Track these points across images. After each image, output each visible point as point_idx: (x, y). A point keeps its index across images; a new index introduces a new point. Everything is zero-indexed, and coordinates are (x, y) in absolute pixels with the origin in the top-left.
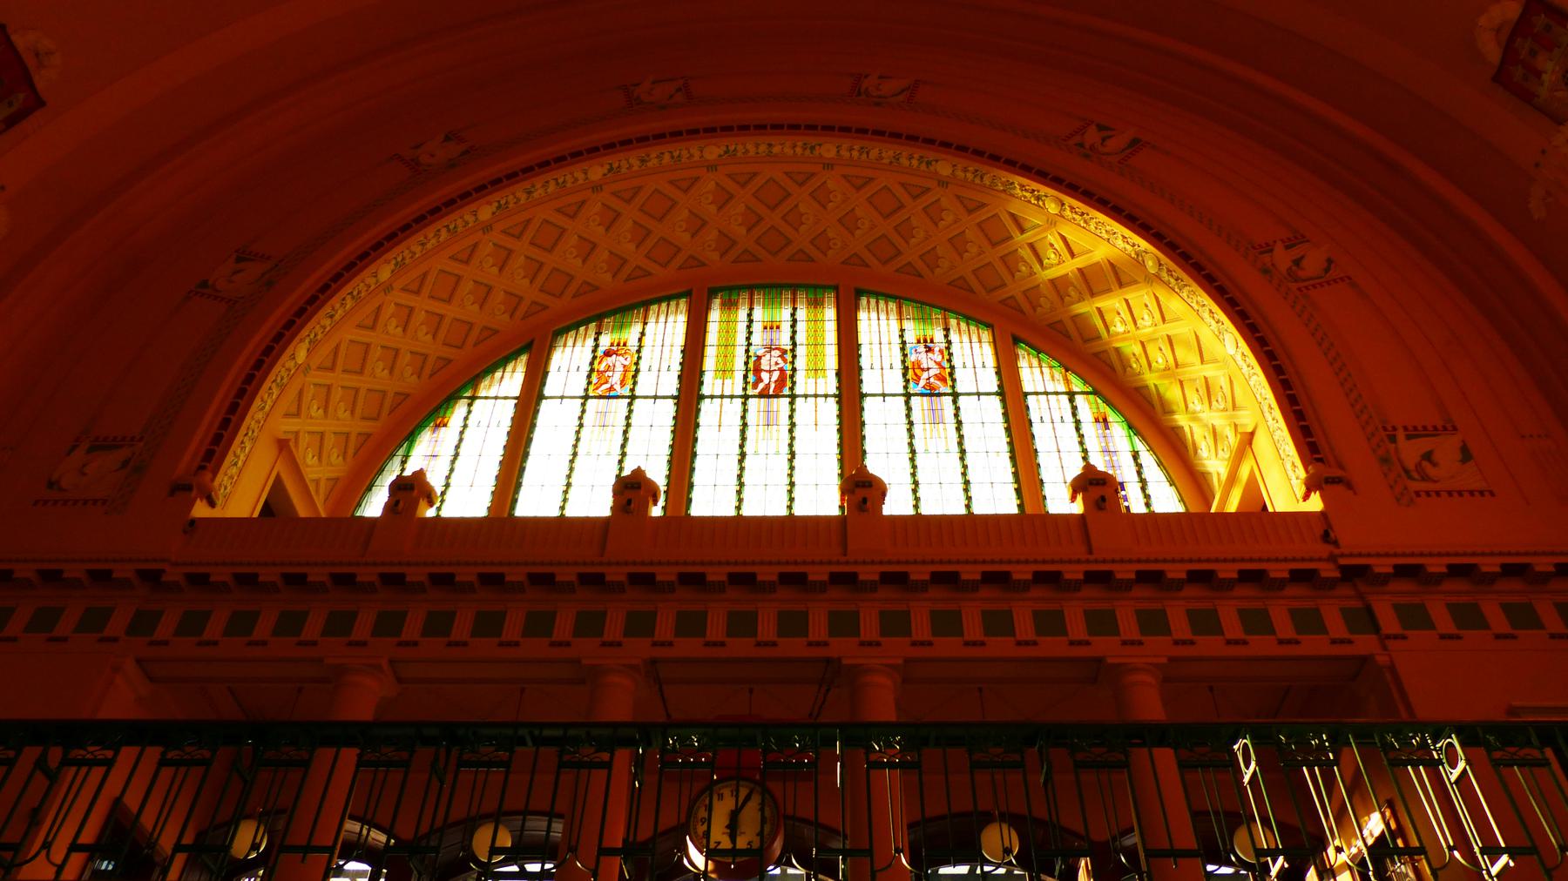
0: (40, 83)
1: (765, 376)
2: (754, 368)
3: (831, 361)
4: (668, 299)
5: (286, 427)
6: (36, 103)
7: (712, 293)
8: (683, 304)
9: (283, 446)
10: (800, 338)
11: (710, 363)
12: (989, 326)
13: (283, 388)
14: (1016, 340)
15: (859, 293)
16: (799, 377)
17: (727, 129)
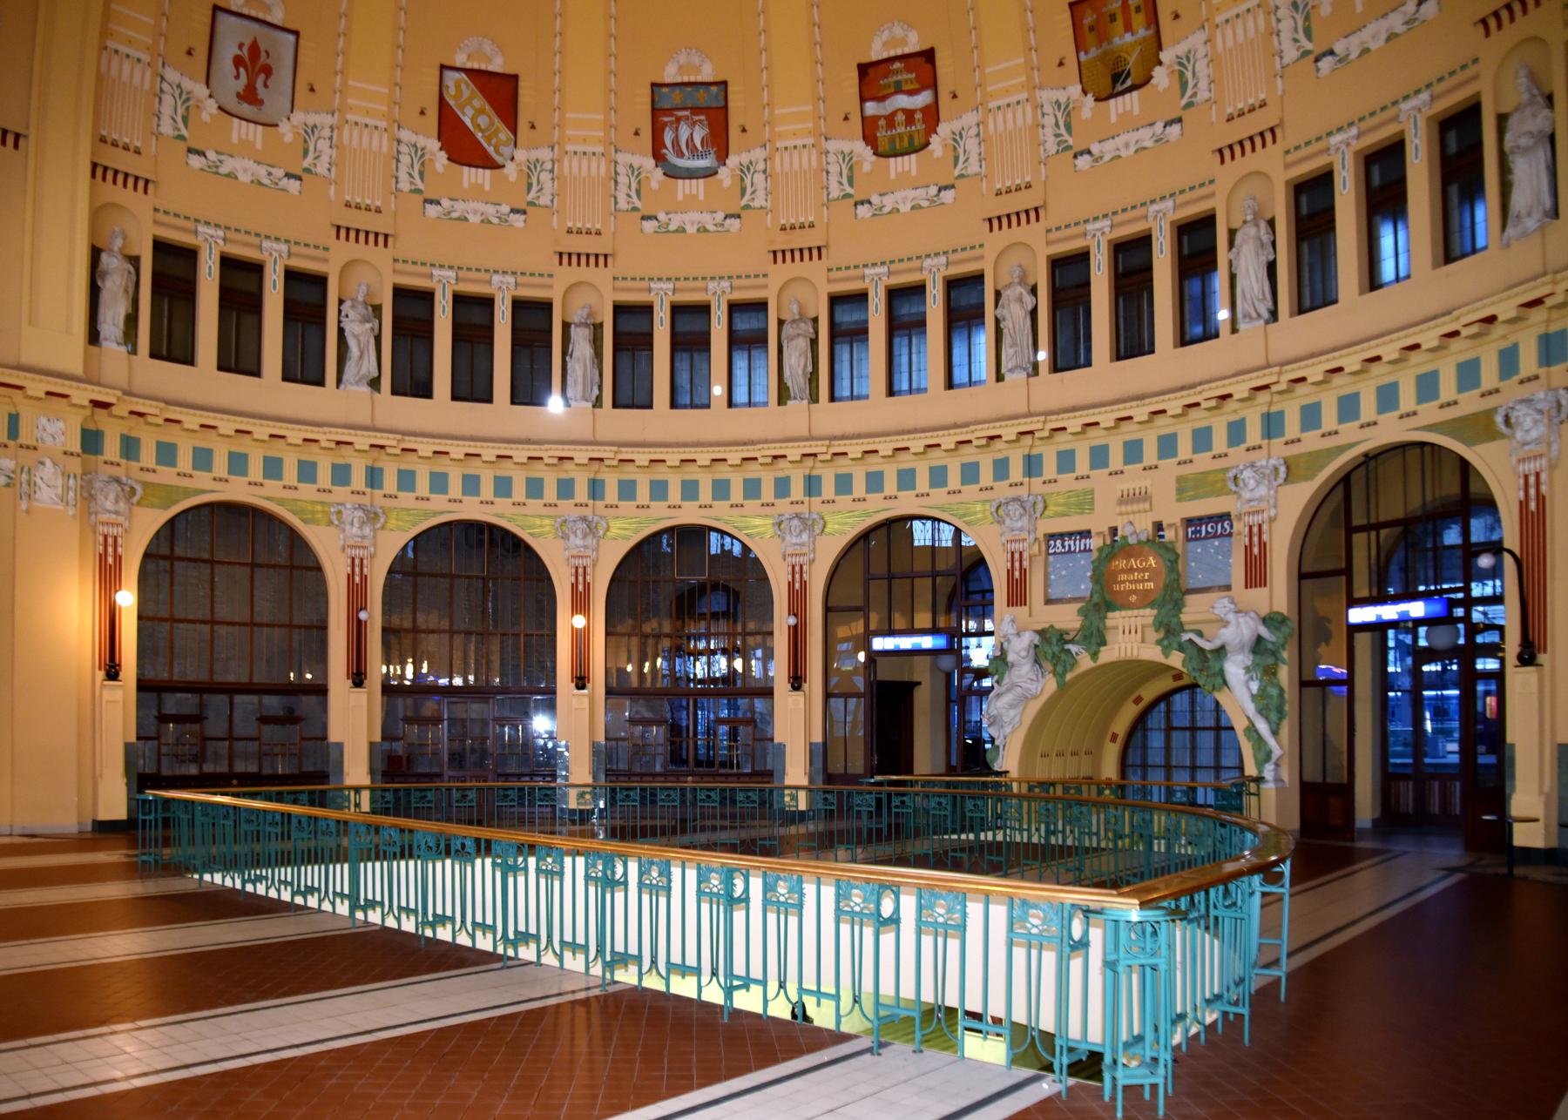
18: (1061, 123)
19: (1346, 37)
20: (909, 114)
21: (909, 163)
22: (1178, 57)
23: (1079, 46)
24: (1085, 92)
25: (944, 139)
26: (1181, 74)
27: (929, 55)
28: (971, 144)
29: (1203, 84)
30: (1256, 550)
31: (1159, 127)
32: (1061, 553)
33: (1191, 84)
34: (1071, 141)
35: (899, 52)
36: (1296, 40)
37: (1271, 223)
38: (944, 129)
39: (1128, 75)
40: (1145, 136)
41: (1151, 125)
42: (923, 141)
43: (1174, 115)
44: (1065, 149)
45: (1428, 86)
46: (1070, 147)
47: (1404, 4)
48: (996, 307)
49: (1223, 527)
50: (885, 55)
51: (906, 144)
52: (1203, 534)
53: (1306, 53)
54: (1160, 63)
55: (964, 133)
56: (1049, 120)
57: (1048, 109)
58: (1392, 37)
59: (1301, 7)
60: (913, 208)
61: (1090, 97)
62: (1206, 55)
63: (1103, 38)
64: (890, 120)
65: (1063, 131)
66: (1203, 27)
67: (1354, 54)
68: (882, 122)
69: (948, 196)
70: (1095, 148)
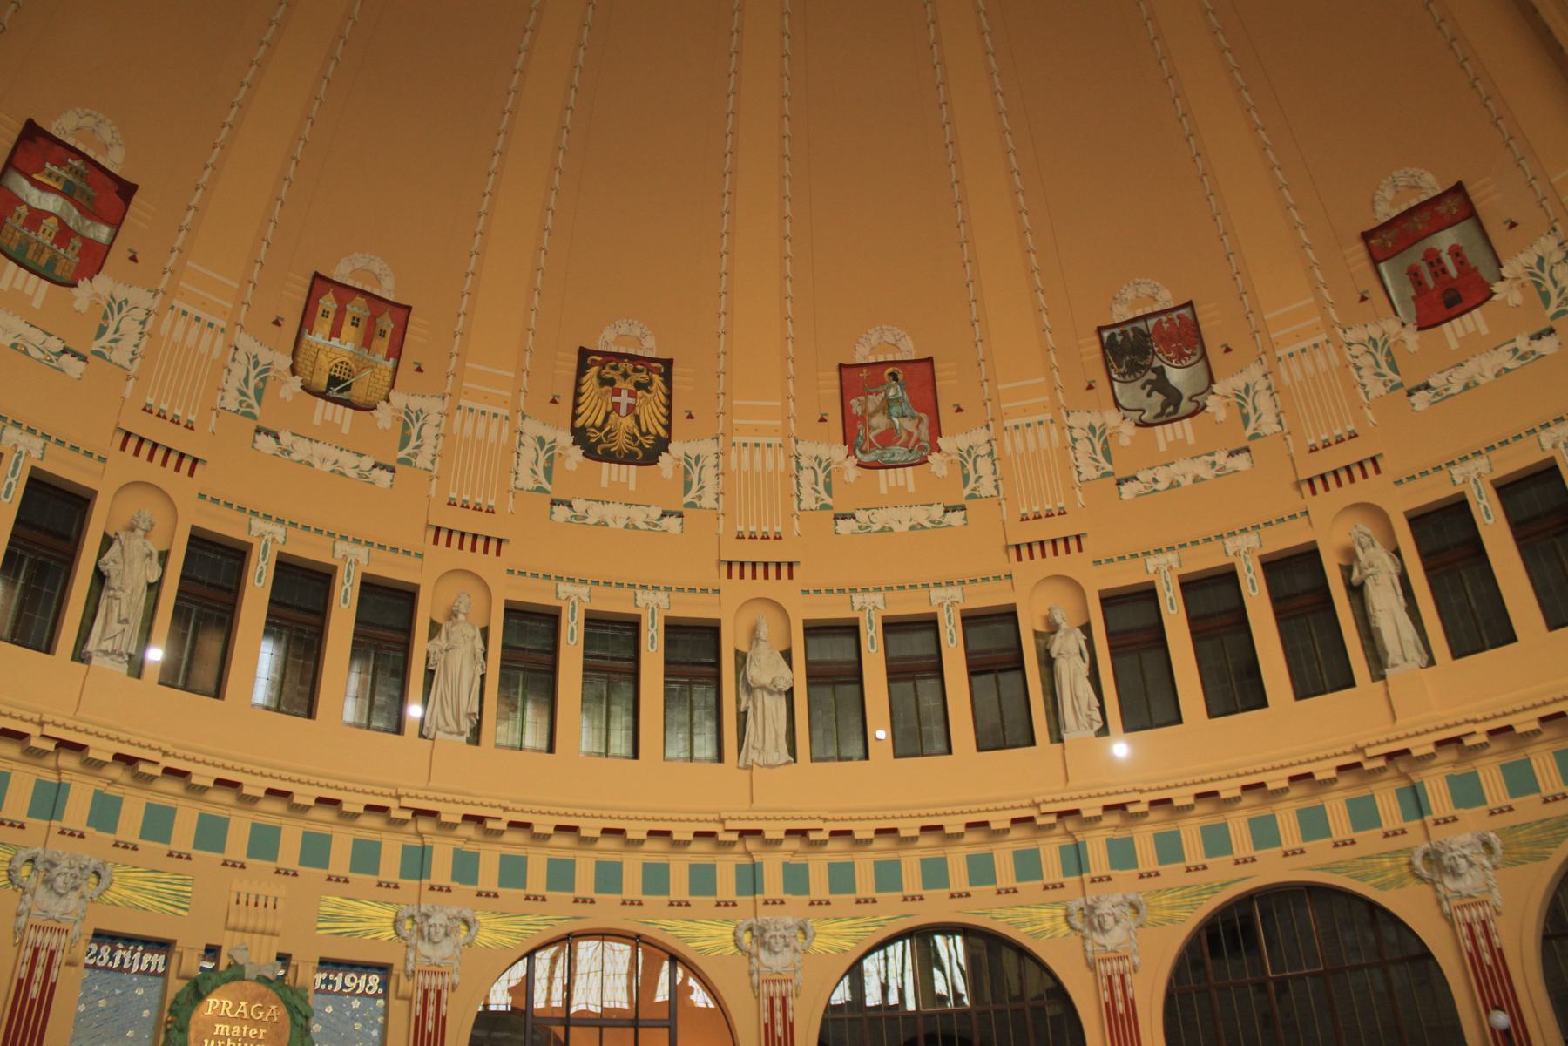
18: (252, 384)
19: (587, 500)
20: (65, 234)
21: (38, 289)
22: (407, 407)
23: (306, 321)
24: (294, 371)
25: (98, 295)
26: (406, 426)
27: (127, 191)
28: (130, 327)
29: (427, 451)
30: (430, 1025)
31: (367, 463)
32: (106, 969)
33: (413, 443)
34: (257, 411)
35: (91, 153)
36: (534, 472)
37: (485, 632)
38: (103, 284)
39: (348, 388)
40: (348, 461)
41: (361, 455)
42: (68, 276)
43: (392, 462)
44: (245, 414)
45: (668, 589)
46: (253, 417)
47: (648, 506)
48: (100, 556)
49: (367, 982)
50: (71, 141)
51: (43, 261)
52: (338, 987)
53: (540, 490)
54: (388, 400)
55: (125, 309)
56: (239, 371)
57: (241, 356)
58: (631, 526)
59: (547, 447)
60: (14, 346)
61: (296, 382)
62: (438, 426)
63: (335, 332)
64: (36, 217)
65: (251, 392)
66: (443, 399)
67: (591, 520)
68: (23, 210)
69: (73, 366)
70: (286, 438)
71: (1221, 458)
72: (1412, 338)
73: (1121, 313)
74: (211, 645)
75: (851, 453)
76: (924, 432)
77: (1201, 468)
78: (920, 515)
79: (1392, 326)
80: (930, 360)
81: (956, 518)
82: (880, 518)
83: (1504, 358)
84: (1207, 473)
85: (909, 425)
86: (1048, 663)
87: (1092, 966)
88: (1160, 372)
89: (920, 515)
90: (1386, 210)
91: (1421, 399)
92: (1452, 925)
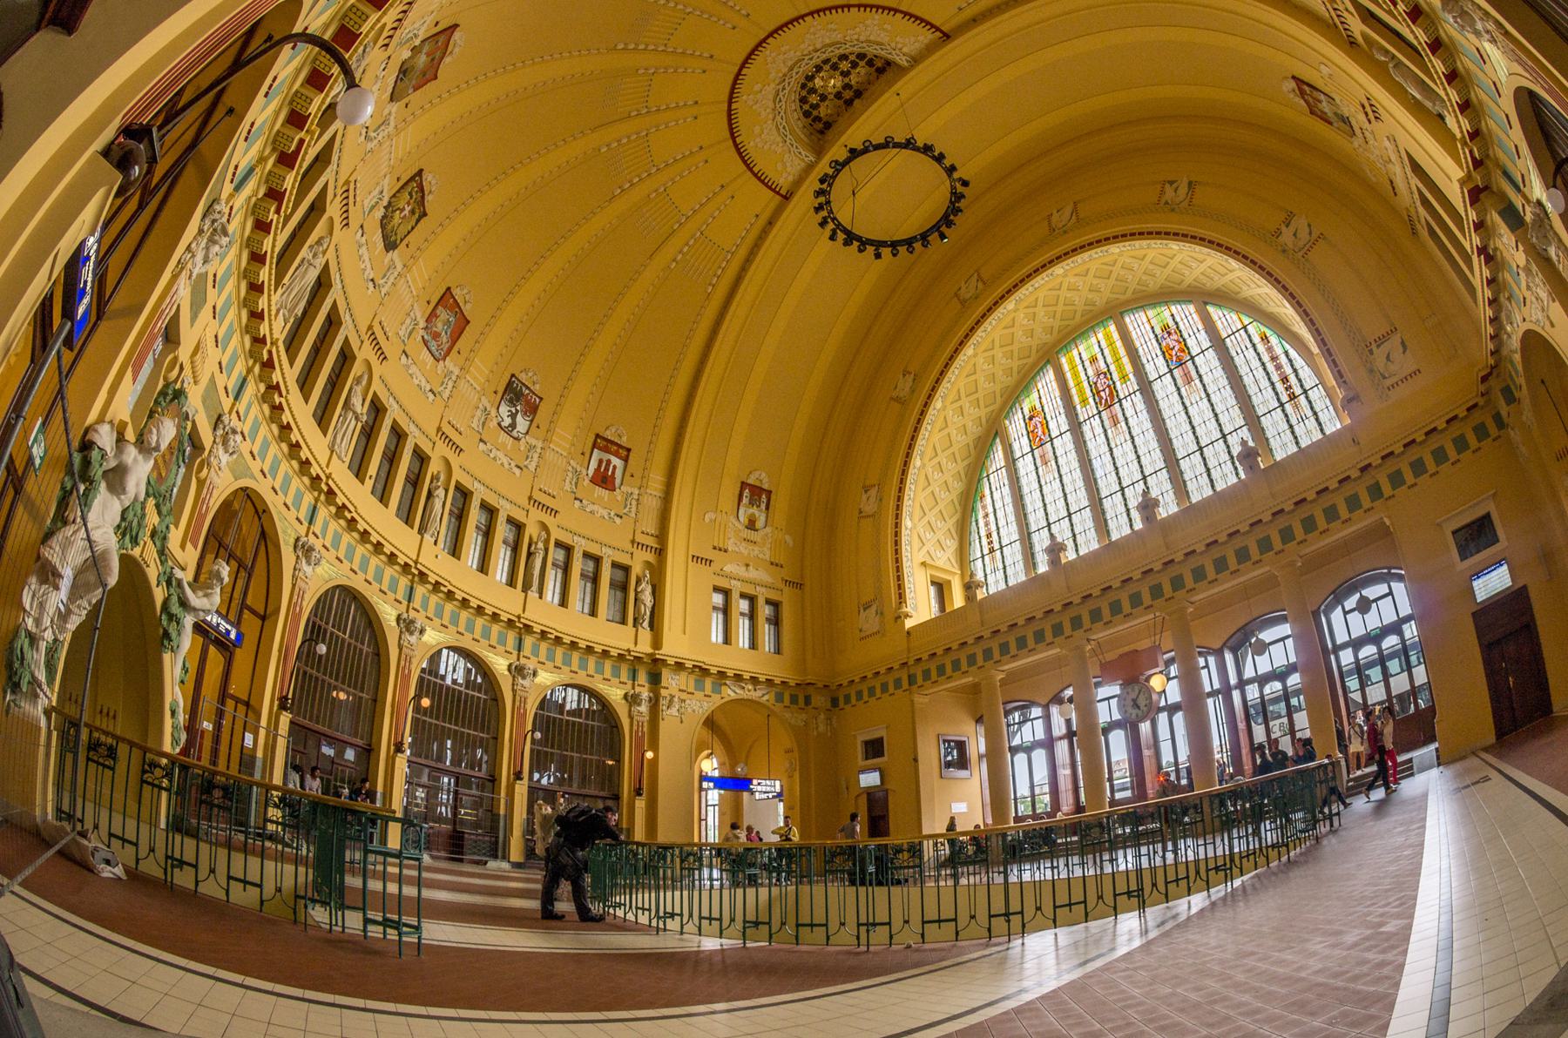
0: (766, 486)
1: (1102, 394)
2: (1096, 393)
3: (1129, 368)
4: (1042, 369)
5: (920, 556)
6: (769, 493)
7: (1058, 353)
8: (1049, 366)
9: (924, 564)
10: (1109, 360)
11: (1076, 400)
12: (1190, 302)
13: (910, 543)
14: (1206, 303)
15: (1122, 314)
16: (1118, 384)
17: (1009, 292)
71: (513, 464)
72: (587, 482)
73: (523, 377)
74: (967, 579)
75: (425, 328)
76: (446, 347)
77: (505, 460)
78: (423, 383)
79: (584, 472)
80: (468, 322)
81: (431, 396)
82: (413, 369)
83: (605, 513)
84: (506, 466)
85: (445, 340)
86: (430, 495)
87: (400, 647)
88: (517, 411)
89: (423, 383)
90: (609, 435)
91: (577, 502)
92: (514, 696)
